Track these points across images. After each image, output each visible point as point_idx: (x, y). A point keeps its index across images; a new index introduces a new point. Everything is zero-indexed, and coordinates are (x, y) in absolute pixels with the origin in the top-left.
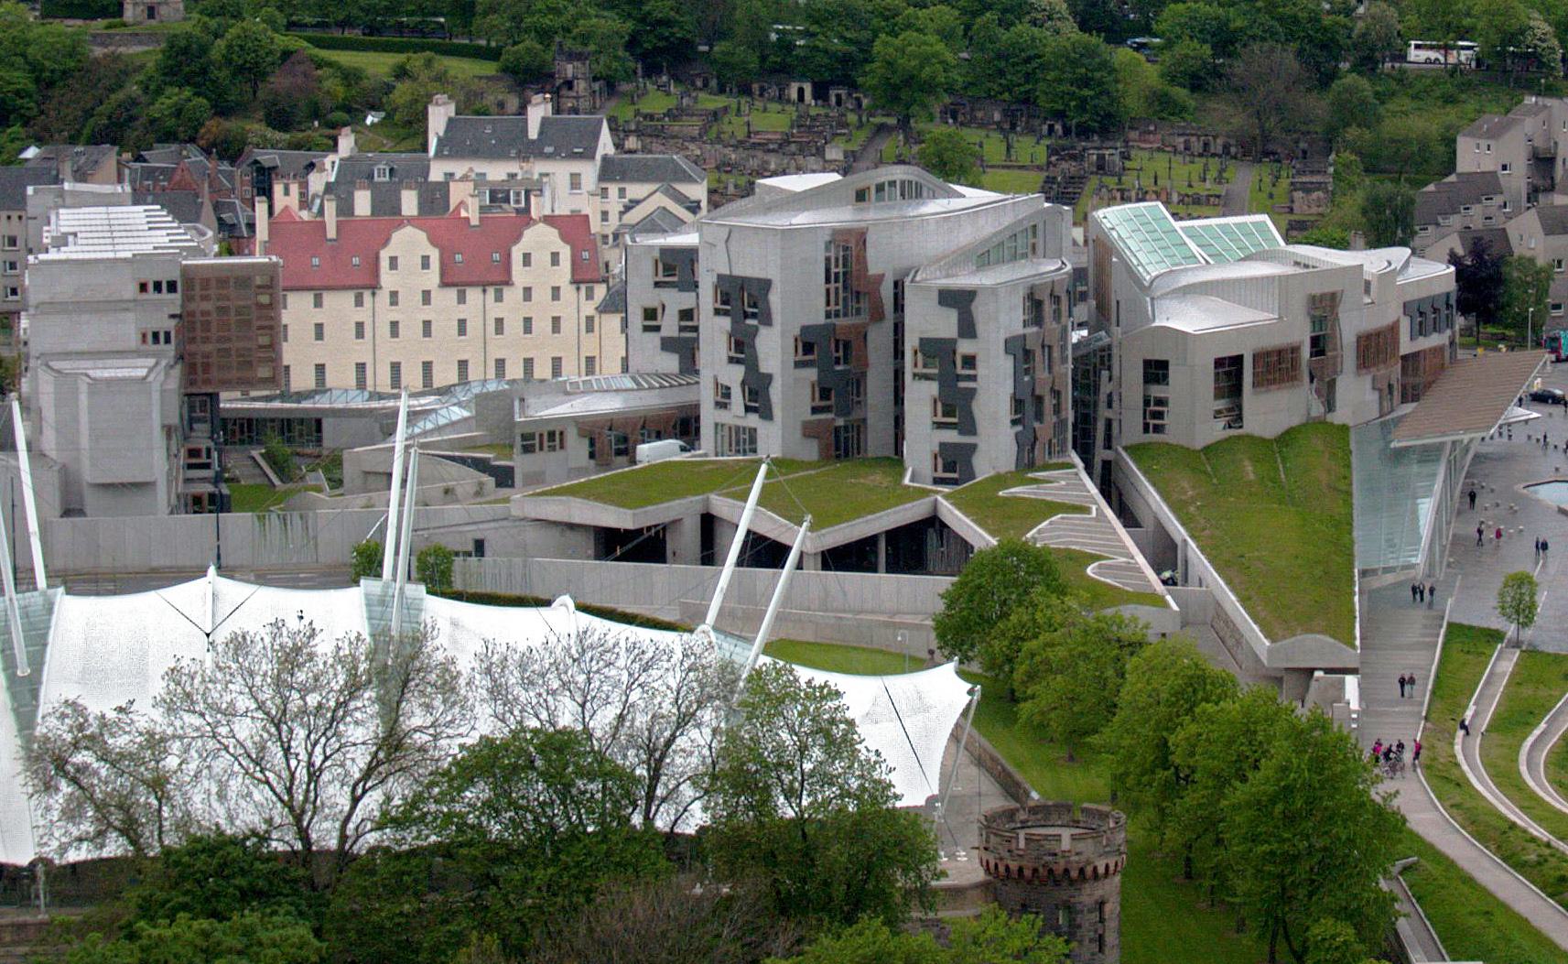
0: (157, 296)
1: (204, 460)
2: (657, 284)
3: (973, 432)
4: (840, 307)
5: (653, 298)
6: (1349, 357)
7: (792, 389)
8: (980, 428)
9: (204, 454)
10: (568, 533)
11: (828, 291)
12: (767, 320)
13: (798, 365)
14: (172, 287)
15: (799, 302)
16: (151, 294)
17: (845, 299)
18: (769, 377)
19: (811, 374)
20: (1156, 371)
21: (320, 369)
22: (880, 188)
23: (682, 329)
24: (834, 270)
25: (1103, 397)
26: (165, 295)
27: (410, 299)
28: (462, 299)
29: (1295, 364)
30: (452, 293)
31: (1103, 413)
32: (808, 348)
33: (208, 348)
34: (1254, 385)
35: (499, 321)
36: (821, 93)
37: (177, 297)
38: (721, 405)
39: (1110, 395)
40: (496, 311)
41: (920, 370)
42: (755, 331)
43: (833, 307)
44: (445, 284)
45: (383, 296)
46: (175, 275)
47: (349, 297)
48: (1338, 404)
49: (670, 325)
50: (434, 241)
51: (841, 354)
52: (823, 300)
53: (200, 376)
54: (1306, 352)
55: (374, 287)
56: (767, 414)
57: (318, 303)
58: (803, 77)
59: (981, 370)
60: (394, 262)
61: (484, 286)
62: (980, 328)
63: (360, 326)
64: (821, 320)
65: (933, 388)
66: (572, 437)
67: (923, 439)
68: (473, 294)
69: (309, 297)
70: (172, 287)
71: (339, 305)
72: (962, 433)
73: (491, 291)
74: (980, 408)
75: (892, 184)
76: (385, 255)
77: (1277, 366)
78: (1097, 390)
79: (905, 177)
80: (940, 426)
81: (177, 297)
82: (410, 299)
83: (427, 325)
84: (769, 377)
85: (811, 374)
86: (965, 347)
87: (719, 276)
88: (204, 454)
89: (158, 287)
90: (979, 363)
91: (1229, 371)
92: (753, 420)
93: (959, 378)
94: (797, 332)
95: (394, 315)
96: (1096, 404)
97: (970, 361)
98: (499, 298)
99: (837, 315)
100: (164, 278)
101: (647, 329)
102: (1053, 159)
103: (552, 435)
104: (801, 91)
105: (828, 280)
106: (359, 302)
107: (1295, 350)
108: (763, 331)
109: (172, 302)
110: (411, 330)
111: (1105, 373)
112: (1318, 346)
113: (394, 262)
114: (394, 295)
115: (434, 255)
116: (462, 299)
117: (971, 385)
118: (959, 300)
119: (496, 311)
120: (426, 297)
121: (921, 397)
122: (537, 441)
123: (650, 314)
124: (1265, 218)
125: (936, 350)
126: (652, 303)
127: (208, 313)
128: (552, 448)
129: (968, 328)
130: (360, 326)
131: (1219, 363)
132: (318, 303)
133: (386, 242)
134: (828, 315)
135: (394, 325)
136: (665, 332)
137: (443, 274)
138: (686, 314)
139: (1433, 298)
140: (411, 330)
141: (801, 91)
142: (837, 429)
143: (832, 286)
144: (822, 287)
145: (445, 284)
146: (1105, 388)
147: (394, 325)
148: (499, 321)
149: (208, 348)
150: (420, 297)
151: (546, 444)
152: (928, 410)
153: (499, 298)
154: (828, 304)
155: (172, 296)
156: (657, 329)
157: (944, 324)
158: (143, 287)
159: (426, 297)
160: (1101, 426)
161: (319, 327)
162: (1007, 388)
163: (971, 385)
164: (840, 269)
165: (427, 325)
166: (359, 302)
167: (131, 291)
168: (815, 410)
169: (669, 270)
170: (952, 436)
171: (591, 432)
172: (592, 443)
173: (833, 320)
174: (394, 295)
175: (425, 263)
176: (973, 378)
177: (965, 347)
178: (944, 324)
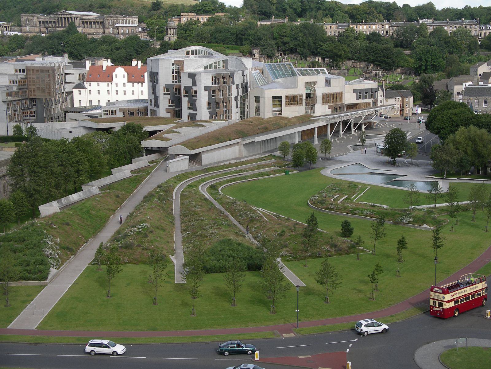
0: (20, 73)
1: (33, 114)
3: (196, 111)
4: (177, 80)
7: (164, 101)
8: (198, 109)
9: (33, 113)
10: (91, 131)
11: (173, 76)
12: (158, 84)
13: (164, 94)
14: (24, 71)
15: (165, 78)
16: (18, 73)
19: (169, 97)
20: (257, 99)
21: (99, 101)
22: (192, 51)
24: (175, 71)
25: (246, 106)
26: (22, 73)
27: (120, 85)
28: (133, 86)
29: (301, 100)
30: (131, 84)
31: (246, 110)
32: (168, 90)
33: (34, 87)
34: (286, 104)
35: (142, 91)
36: (323, 59)
37: (25, 74)
38: (151, 105)
39: (248, 105)
40: (141, 89)
41: (185, 94)
43: (175, 80)
44: (129, 81)
45: (114, 84)
46: (24, 68)
47: (106, 83)
48: (315, 112)
50: (126, 71)
52: (171, 78)
53: (33, 94)
54: (304, 97)
55: (111, 81)
56: (158, 107)
57: (98, 85)
58: (319, 56)
59: (198, 95)
60: (116, 75)
61: (138, 82)
63: (108, 91)
64: (171, 83)
65: (187, 99)
66: (118, 112)
67: (185, 111)
68: (136, 84)
69: (96, 83)
70: (24, 71)
71: (103, 85)
73: (140, 84)
74: (197, 104)
75: (196, 51)
76: (114, 74)
77: (293, 100)
78: (244, 104)
79: (200, 49)
80: (189, 108)
81: (25, 74)
82: (120, 85)
83: (125, 91)
85: (169, 97)
86: (194, 88)
88: (33, 113)
89: (20, 71)
90: (197, 93)
91: (277, 100)
92: (155, 108)
93: (193, 96)
94: (164, 86)
95: (117, 88)
96: (244, 108)
97: (195, 92)
98: (142, 86)
99: (176, 82)
100: (22, 69)
102: (364, 73)
103: (112, 111)
104: (319, 59)
105: (173, 73)
106: (108, 85)
107: (301, 96)
108: (157, 85)
109: (23, 75)
110: (121, 92)
111: (247, 100)
112: (308, 95)
113: (116, 75)
114: (117, 84)
115: (126, 74)
116: (133, 86)
117: (196, 98)
118: (192, 76)
119: (141, 89)
120: (124, 84)
121: (185, 101)
122: (108, 112)
124: (325, 69)
125: (188, 90)
127: (34, 78)
128: (112, 114)
129: (194, 84)
130: (108, 91)
131: (274, 98)
132: (98, 85)
133: (114, 71)
134: (173, 82)
135: (117, 91)
137: (128, 79)
140: (121, 92)
141: (319, 59)
142: (176, 111)
143: (174, 75)
144: (172, 75)
145: (128, 82)
146: (247, 104)
147: (117, 91)
148: (142, 91)
149: (34, 87)
150: (123, 85)
151: (111, 113)
152: (187, 104)
153: (142, 86)
154: (173, 79)
155: (23, 73)
158: (16, 71)
159: (124, 84)
160: (246, 113)
161: (99, 91)
162: (206, 99)
163: (196, 98)
164: (177, 71)
165: (125, 91)
166: (108, 85)
167: (13, 72)
168: (169, 106)
170: (191, 111)
171: (124, 110)
172: (124, 114)
174: (117, 84)
175: (124, 76)
176: (196, 96)
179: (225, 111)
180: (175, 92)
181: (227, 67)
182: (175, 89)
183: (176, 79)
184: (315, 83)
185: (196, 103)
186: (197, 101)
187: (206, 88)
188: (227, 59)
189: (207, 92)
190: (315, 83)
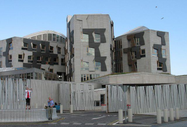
2: (23, 49)
5: (21, 52)
18: (105, 57)
23: (29, 61)
42: (98, 44)
49: (26, 60)
72: (163, 71)
84: (105, 57)
87: (84, 30)
101: (19, 61)
108: (102, 44)
123: (20, 56)
126: (22, 54)
129: (164, 43)
136: (24, 62)
138: (29, 57)
156: (22, 61)
157: (158, 41)
169: (25, 44)
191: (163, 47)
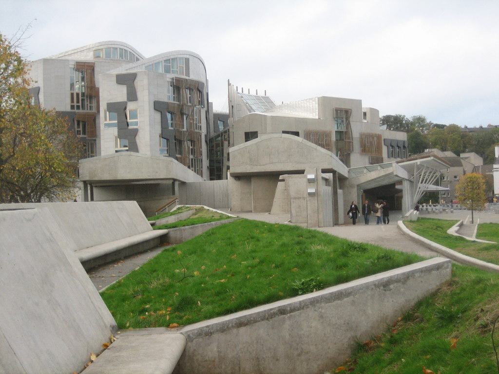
4: (80, 104)
6: (356, 146)
17: (83, 100)
25: (225, 155)
41: (108, 122)
43: (75, 104)
51: (81, 129)
52: (69, 100)
54: (334, 138)
62: (139, 95)
64: (68, 109)
65: (114, 131)
99: (78, 107)
112: (339, 133)
117: (135, 127)
129: (132, 96)
134: (72, 107)
139: (398, 141)
152: (113, 144)
154: (72, 101)
157: (119, 94)
173: (76, 110)
177: (131, 106)
178: (119, 94)
179: (192, 159)
180: (76, 129)
181: (188, 74)
182: (76, 122)
183: (78, 102)
184: (347, 113)
185: (137, 138)
186: (139, 133)
187: (158, 106)
188: (188, 57)
189: (158, 116)
190: (347, 113)
191: (131, 106)
